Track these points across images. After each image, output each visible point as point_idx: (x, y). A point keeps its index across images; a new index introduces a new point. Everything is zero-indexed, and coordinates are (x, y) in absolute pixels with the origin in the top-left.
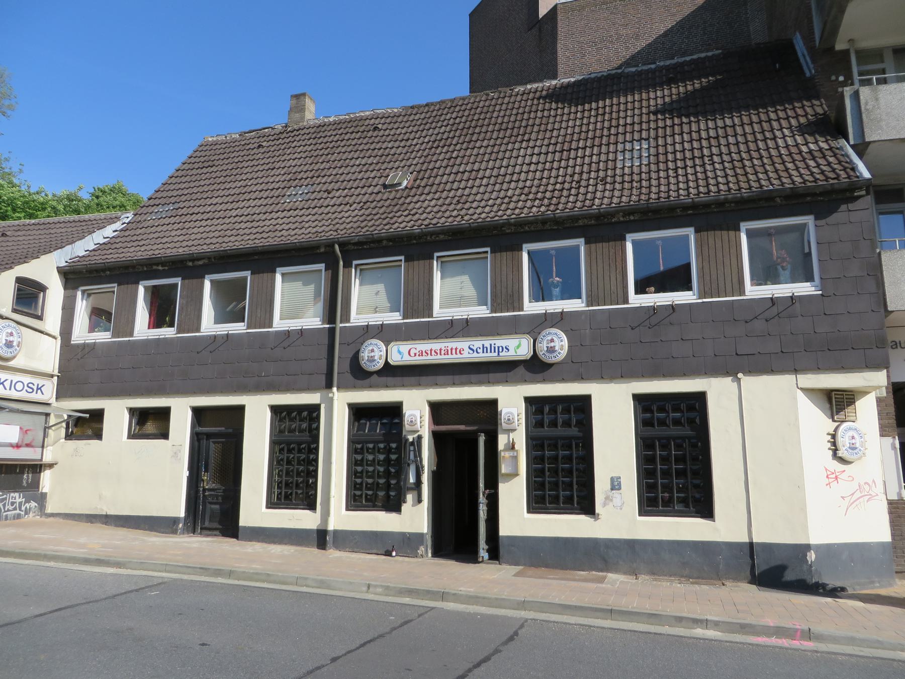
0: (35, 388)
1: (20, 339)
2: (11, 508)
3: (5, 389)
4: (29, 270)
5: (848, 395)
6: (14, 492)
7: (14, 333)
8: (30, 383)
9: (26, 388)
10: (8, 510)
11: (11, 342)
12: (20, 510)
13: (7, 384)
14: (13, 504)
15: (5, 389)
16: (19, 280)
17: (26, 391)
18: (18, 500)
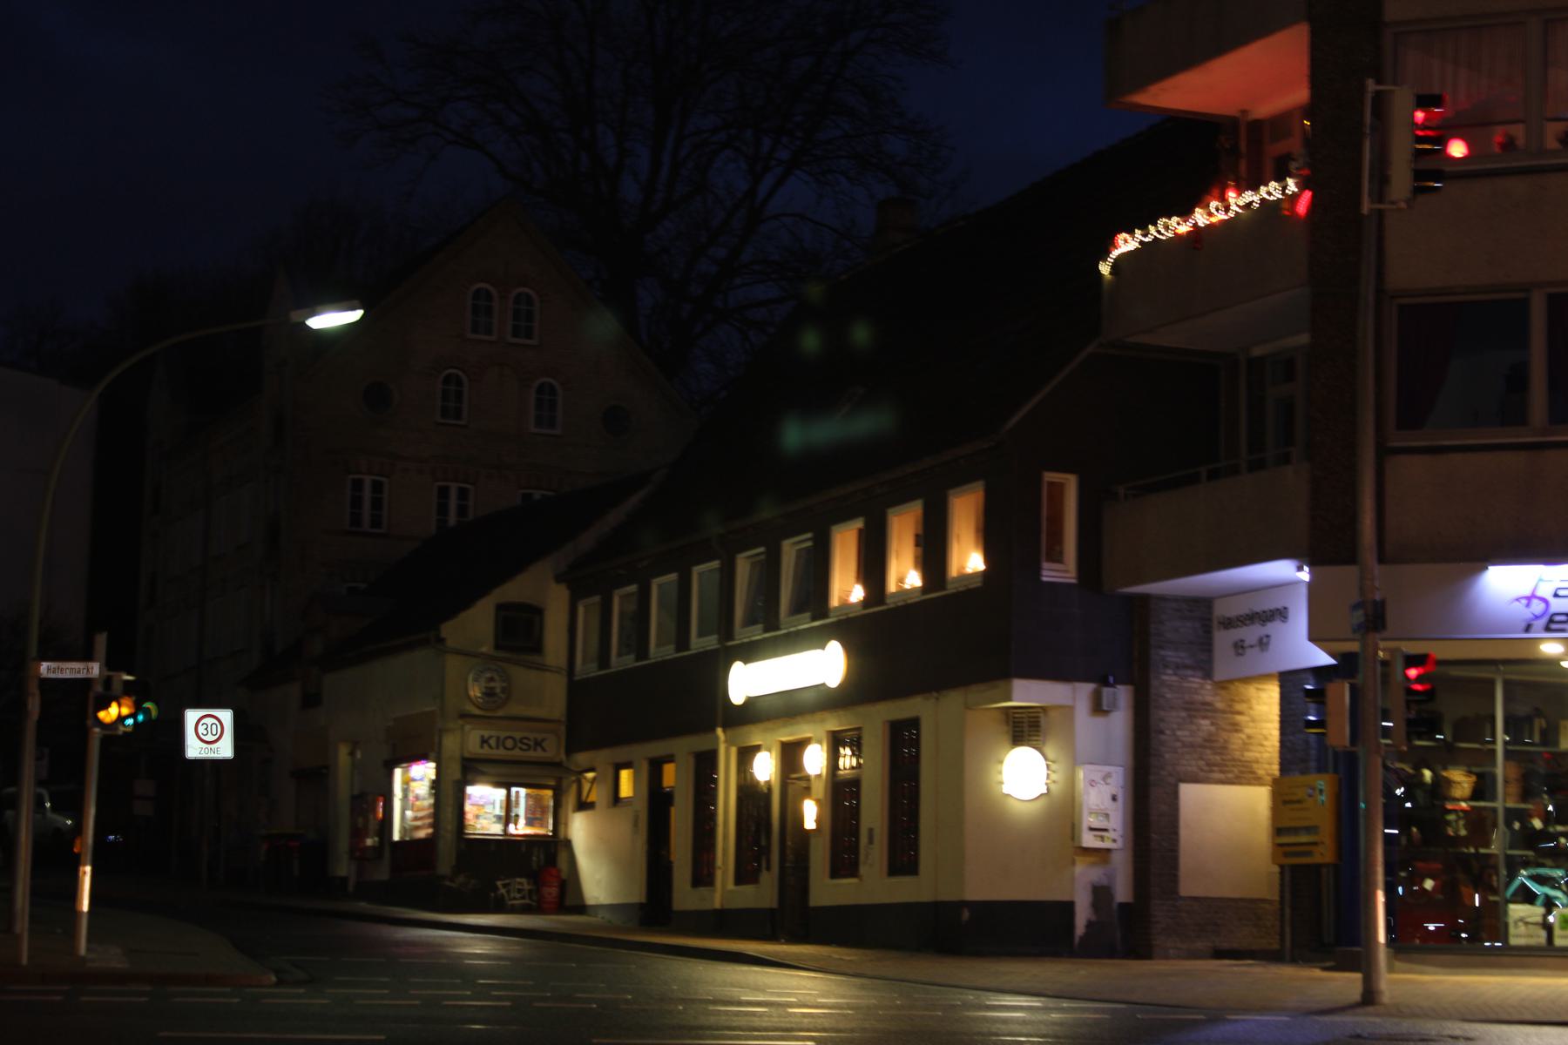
0: (531, 743)
1: (504, 684)
2: (518, 896)
3: (490, 747)
4: (513, 591)
5: (1029, 713)
6: (521, 877)
7: (496, 677)
8: (526, 738)
9: (520, 745)
10: (515, 899)
11: (492, 688)
12: (530, 898)
13: (493, 742)
14: (519, 891)
15: (490, 747)
16: (500, 607)
17: (521, 749)
18: (527, 887)
